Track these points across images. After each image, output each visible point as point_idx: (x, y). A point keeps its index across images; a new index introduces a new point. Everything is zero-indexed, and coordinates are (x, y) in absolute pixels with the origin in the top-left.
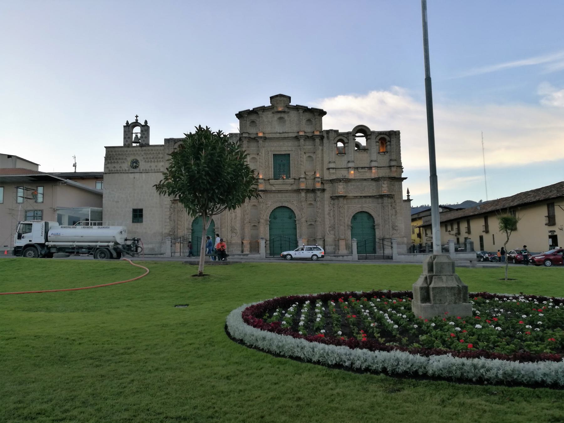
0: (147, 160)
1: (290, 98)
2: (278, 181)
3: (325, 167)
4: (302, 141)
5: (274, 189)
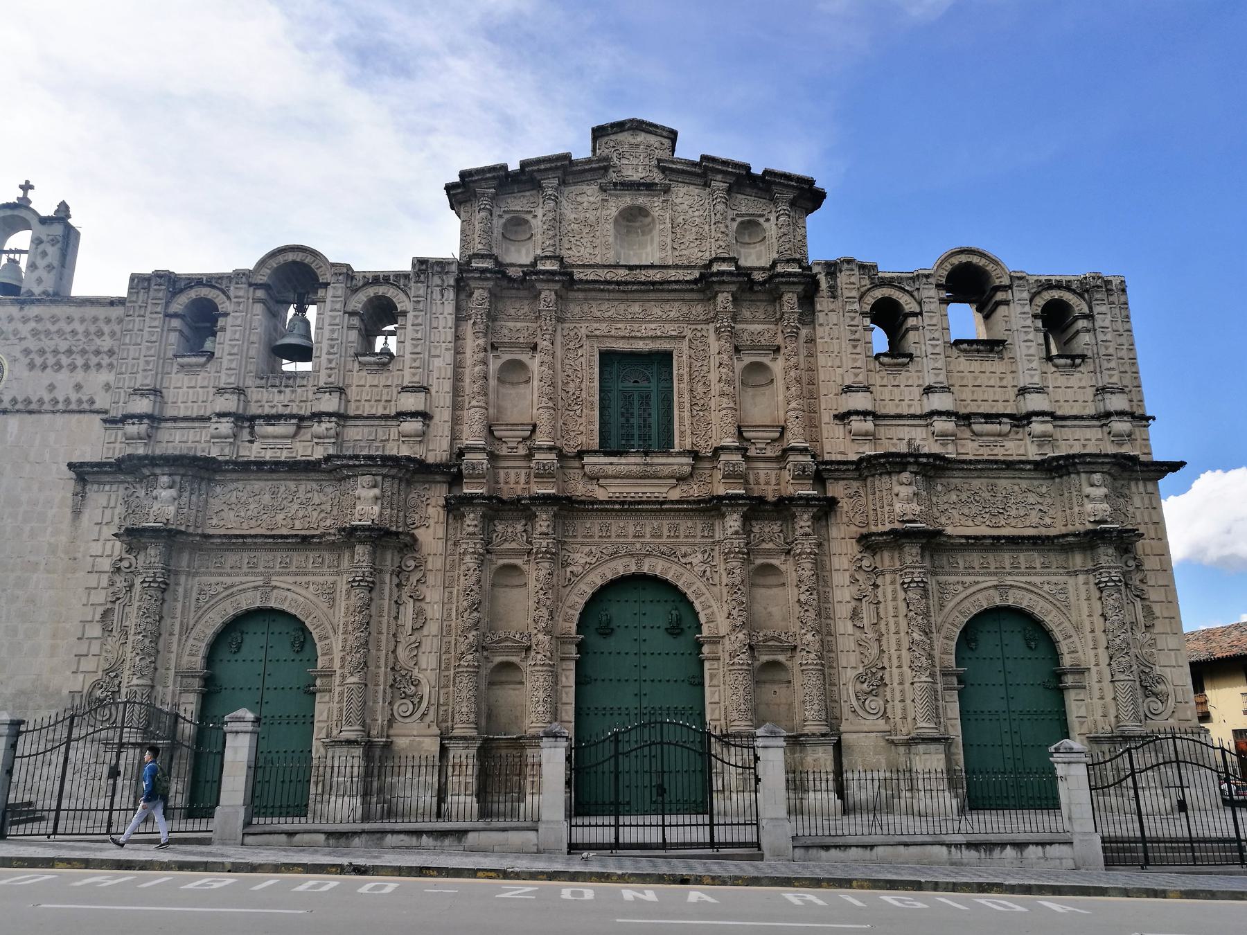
0: (38, 361)
1: (673, 135)
2: (623, 460)
3: (831, 403)
4: (724, 299)
5: (601, 494)
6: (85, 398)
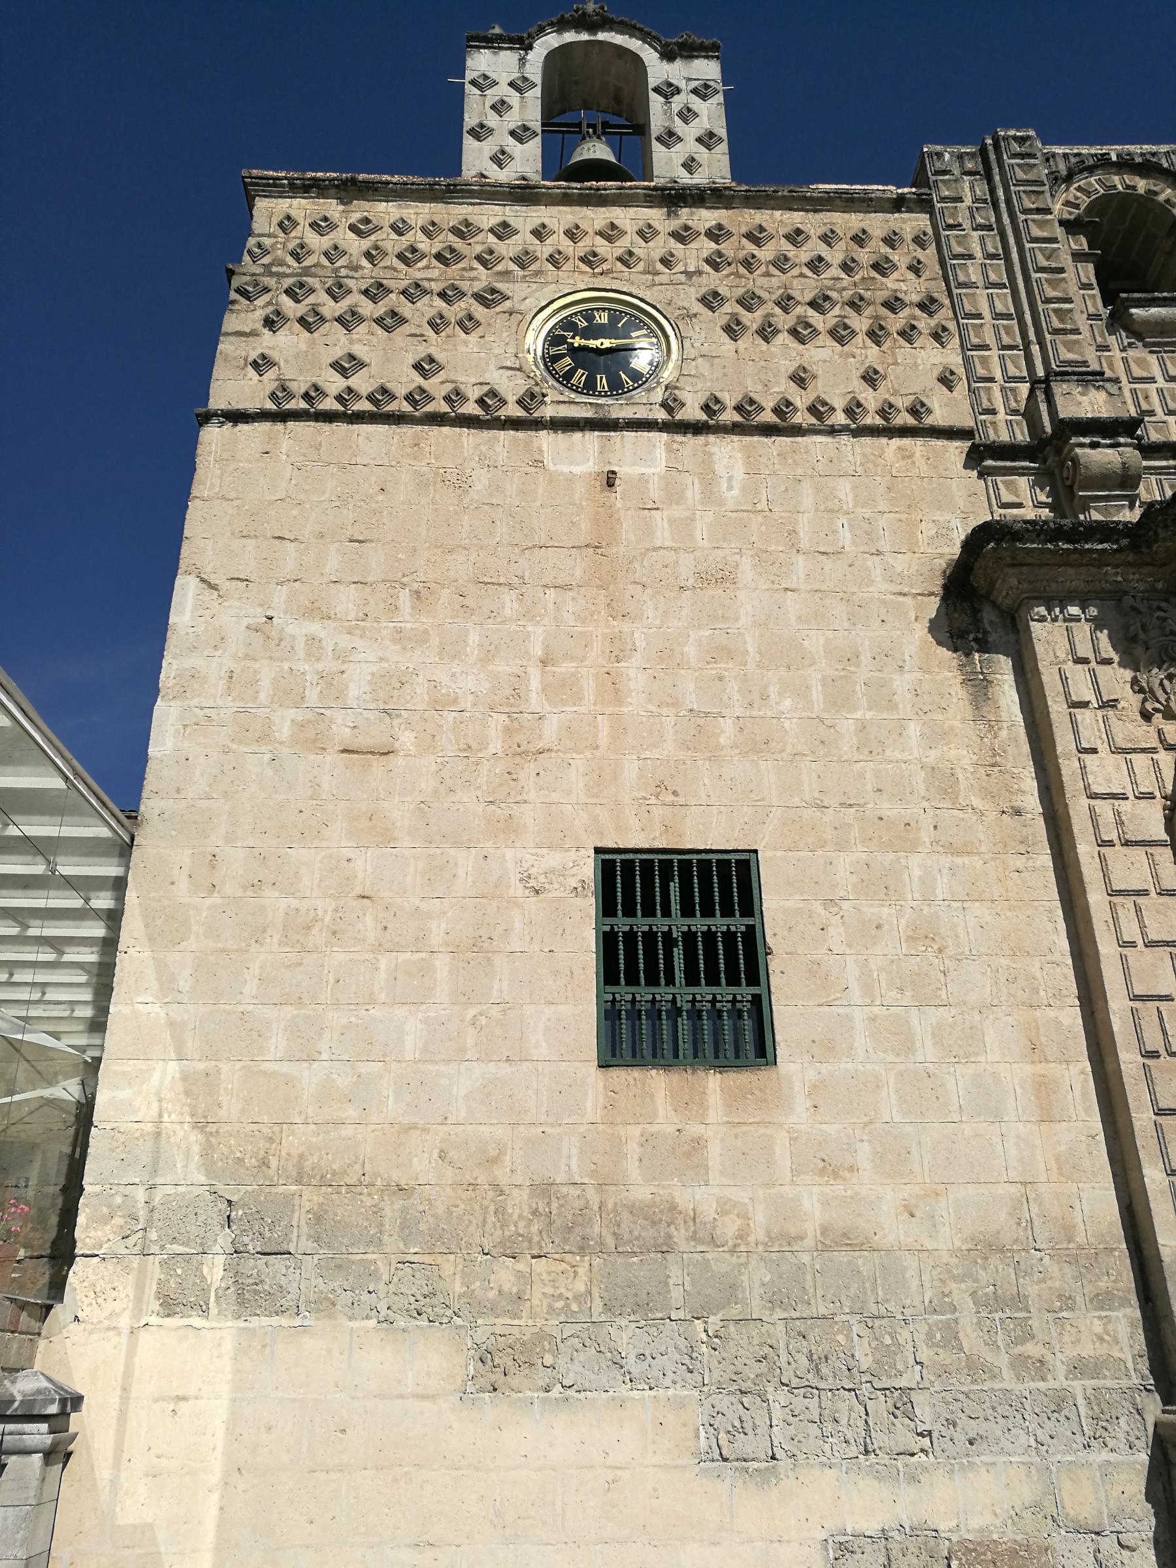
6: (902, 403)
